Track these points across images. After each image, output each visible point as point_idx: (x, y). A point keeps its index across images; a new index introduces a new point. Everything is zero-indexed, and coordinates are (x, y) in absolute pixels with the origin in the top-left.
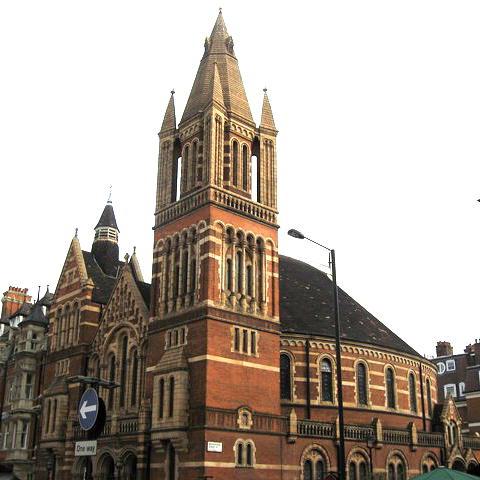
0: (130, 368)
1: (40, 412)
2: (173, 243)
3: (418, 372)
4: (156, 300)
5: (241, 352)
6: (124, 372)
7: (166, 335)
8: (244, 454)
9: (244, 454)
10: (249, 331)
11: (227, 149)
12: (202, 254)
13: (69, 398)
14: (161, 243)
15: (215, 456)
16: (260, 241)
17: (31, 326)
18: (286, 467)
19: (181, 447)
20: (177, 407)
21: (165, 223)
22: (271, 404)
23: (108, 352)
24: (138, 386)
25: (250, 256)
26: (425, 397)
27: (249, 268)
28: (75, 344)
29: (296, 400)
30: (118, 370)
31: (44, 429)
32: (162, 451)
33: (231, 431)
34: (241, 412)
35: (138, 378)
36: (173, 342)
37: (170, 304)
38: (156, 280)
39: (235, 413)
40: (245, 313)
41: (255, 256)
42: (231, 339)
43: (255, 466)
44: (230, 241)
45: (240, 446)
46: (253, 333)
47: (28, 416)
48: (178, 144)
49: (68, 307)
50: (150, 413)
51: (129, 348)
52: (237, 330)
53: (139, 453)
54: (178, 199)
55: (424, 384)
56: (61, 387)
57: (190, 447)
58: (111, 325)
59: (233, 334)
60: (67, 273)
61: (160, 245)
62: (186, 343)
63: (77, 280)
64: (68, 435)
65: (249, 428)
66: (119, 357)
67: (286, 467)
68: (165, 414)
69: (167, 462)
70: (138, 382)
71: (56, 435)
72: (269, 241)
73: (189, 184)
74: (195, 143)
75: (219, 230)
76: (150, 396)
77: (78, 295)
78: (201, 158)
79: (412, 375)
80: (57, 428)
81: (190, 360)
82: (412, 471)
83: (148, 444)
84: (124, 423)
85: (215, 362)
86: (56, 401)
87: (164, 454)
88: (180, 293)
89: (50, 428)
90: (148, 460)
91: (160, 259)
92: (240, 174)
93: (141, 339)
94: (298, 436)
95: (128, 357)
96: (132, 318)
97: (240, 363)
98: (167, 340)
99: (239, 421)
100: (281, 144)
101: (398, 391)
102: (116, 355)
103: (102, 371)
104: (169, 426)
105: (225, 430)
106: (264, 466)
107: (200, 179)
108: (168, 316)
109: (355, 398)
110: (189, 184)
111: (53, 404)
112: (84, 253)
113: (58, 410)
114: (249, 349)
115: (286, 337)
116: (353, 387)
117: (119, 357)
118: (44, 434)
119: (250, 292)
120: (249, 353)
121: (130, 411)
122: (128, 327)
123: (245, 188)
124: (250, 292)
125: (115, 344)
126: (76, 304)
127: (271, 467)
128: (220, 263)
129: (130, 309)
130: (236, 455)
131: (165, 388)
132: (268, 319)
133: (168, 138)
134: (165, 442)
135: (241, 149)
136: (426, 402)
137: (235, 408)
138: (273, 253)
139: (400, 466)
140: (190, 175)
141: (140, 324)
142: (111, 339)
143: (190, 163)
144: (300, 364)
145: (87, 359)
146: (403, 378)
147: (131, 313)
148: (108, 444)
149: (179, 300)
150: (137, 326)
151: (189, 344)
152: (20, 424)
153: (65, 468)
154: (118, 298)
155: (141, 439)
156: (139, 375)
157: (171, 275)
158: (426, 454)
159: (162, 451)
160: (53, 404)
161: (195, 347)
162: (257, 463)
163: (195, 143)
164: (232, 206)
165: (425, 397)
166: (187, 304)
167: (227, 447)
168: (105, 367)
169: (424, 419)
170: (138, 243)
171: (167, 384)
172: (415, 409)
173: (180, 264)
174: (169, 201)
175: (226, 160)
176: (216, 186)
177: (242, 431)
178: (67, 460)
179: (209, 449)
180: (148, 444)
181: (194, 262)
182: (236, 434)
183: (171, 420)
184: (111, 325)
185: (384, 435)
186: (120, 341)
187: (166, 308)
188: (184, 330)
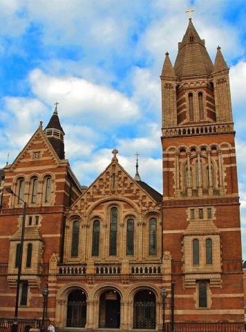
58: (95, 197)
74: (200, 94)
77: (53, 170)
125: (99, 211)
129: (126, 189)
142: (96, 207)
147: (131, 191)
150: (137, 201)
183: (209, 266)
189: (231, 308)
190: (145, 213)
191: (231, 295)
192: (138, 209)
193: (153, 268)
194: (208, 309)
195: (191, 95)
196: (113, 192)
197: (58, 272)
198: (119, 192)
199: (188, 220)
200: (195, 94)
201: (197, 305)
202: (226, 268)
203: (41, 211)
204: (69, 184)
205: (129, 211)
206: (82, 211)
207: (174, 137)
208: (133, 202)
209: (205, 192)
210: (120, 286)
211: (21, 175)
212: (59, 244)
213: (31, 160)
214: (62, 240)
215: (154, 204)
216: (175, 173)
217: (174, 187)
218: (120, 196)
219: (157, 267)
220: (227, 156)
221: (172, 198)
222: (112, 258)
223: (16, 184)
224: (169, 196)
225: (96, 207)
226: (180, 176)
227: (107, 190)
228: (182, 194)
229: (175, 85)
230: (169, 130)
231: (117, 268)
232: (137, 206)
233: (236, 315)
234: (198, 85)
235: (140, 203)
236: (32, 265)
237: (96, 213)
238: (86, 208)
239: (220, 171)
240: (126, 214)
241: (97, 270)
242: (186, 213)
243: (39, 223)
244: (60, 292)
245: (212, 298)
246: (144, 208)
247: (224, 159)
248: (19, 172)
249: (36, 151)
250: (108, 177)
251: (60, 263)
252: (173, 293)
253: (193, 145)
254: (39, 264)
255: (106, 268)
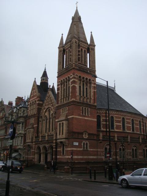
0: (51, 120)
1: (26, 134)
2: (63, 81)
3: (142, 120)
4: (58, 99)
5: (84, 114)
6: (50, 121)
7: (61, 110)
8: (85, 146)
9: (85, 146)
10: (87, 108)
11: (79, 51)
12: (71, 84)
13: (34, 130)
14: (59, 81)
15: (76, 146)
16: (90, 80)
17: (23, 108)
18: (99, 150)
19: (66, 144)
20: (64, 132)
21: (61, 75)
22: (94, 131)
23: (45, 115)
24: (54, 126)
25: (87, 85)
26: (144, 128)
27: (87, 89)
28: (35, 113)
29: (102, 129)
30: (48, 121)
31: (27, 139)
32: (61, 145)
33: (81, 139)
34: (84, 133)
35: (54, 123)
36: (63, 112)
37: (62, 100)
38: (58, 93)
39: (82, 134)
40: (85, 102)
41: (88, 85)
42: (81, 111)
43: (89, 149)
44: (80, 80)
45: (84, 143)
46: (88, 109)
47: (23, 135)
48: (64, 50)
49: (33, 102)
50: (56, 134)
52: (83, 108)
53: (54, 146)
54: (64, 67)
55: (144, 124)
56: (30, 127)
58: (45, 107)
59: (81, 109)
60: (33, 92)
61: (59, 82)
62: (67, 112)
63: (35, 94)
64: (34, 141)
65: (87, 138)
66: (48, 117)
67: (99, 150)
68: (61, 134)
69: (62, 148)
70: (54, 124)
71: (30, 141)
72: (93, 80)
73: (68, 63)
74: (69, 50)
75: (76, 77)
76: (56, 129)
77: (36, 98)
78: (71, 55)
79: (140, 121)
80: (30, 139)
81: (68, 117)
82: (140, 151)
83: (56, 143)
84: (49, 137)
85: (76, 118)
86: (30, 131)
87: (61, 146)
88: (65, 97)
89: (29, 139)
90: (56, 148)
91: (59, 86)
92: (83, 59)
93: (54, 111)
94: (103, 140)
95: (51, 117)
96: (52, 105)
97: (83, 118)
99: (84, 136)
100: (96, 49)
101: (135, 126)
102: (47, 116)
103: (43, 121)
104: (62, 138)
105: (79, 139)
106: (92, 150)
107: (71, 61)
108: (62, 104)
109: (121, 128)
110: (68, 63)
111: (29, 131)
112: (38, 86)
113: (31, 133)
114: (87, 114)
115: (100, 110)
116: (121, 125)
117: (48, 117)
118: (27, 140)
119: (87, 96)
120: (87, 115)
121: (51, 133)
122: (50, 108)
123: (85, 63)
124: (87, 96)
126: (35, 101)
127: (94, 150)
128: (77, 87)
130: (83, 146)
131: (61, 126)
132: (93, 104)
133: (61, 49)
134: (61, 142)
135: (83, 51)
136: (145, 130)
137: (82, 132)
138: (95, 84)
139: (136, 149)
140: (68, 60)
141: (54, 107)
143: (68, 56)
144: (104, 118)
145: (39, 118)
146: (137, 122)
147: (51, 103)
148: (45, 143)
149: (65, 99)
150: (53, 107)
152: (20, 137)
153: (33, 150)
154: (47, 99)
155: (54, 142)
156: (54, 122)
157: (63, 91)
158: (144, 146)
159: (61, 145)
160: (29, 131)
162: (90, 148)
163: (69, 50)
164: (81, 69)
165: (144, 128)
166: (67, 100)
167: (80, 144)
168: (44, 120)
169: (144, 135)
170: (53, 81)
171: (61, 125)
172: (141, 132)
173: (65, 88)
174: (62, 68)
175: (79, 55)
176: (75, 63)
177: (84, 139)
178: (33, 148)
179: (74, 144)
180: (56, 143)
181: (69, 87)
182: (83, 140)
184: (45, 107)
185: (131, 140)
186: (48, 112)
187: (61, 101)
188: (66, 108)
194: (64, 156)
195: (67, 52)
198: (49, 104)
201: (62, 154)
220: (71, 81)
221: (58, 105)
244: (36, 148)
245: (66, 151)
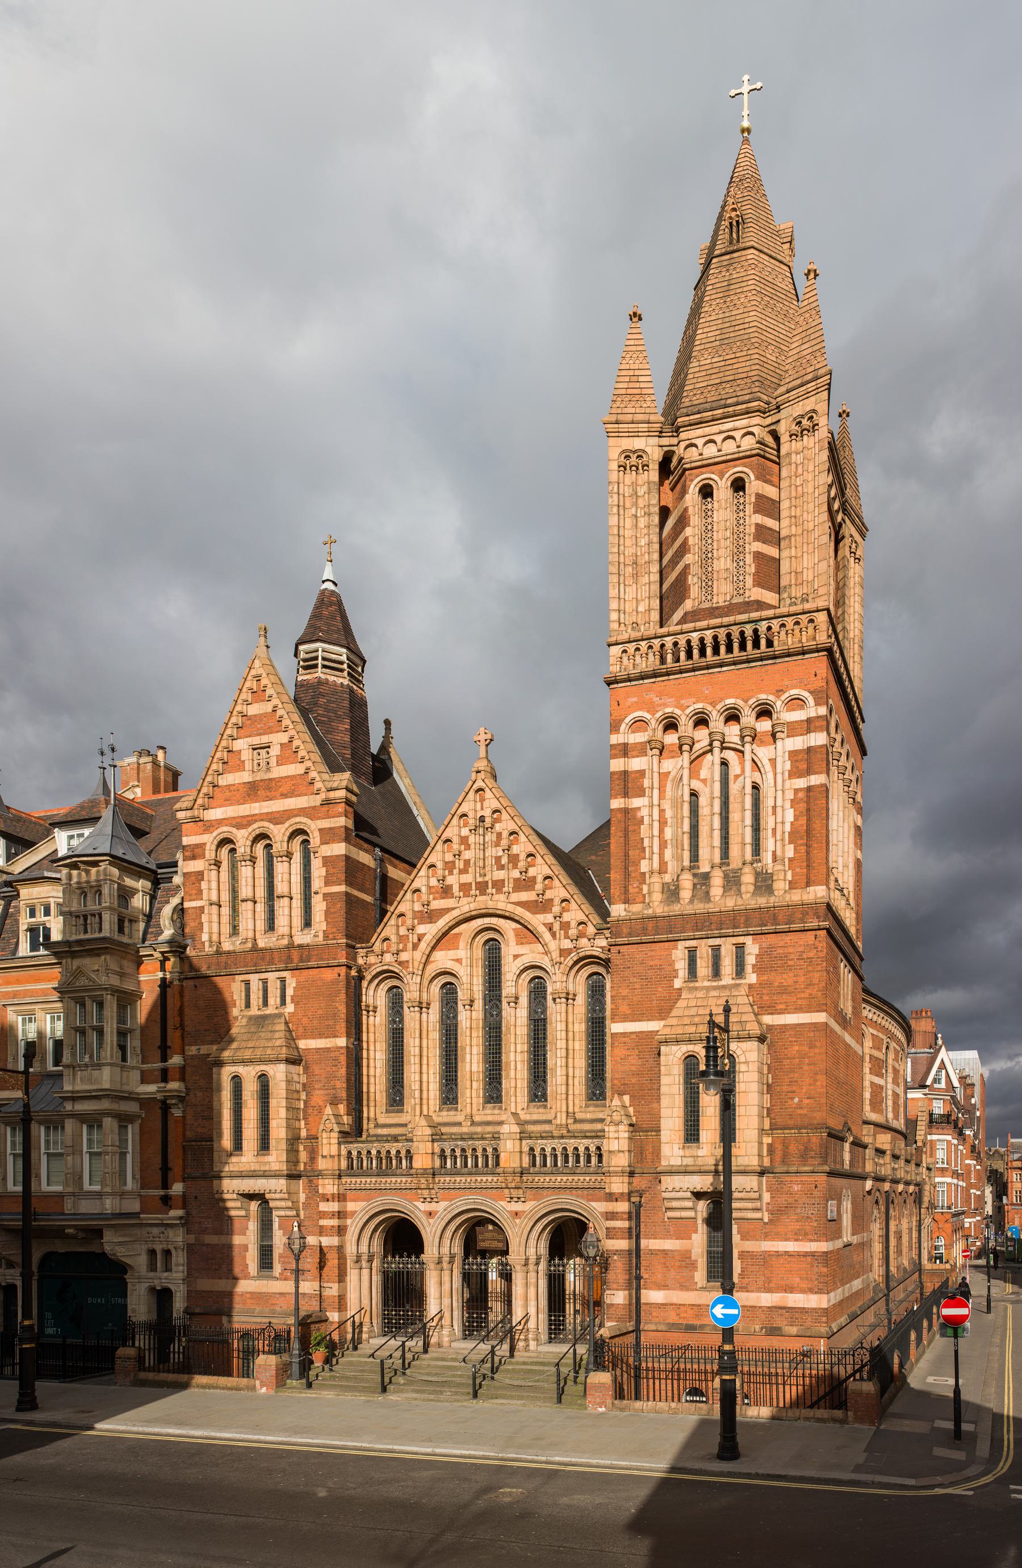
32: (691, 1214)
51: (510, 969)
57: (778, 1212)
58: (437, 904)
62: (752, 978)
74: (738, 485)
77: (309, 812)
81: (768, 1019)
96: (525, 896)
98: (681, 966)
125: (452, 954)
129: (516, 874)
142: (441, 940)
147: (525, 883)
150: (549, 918)
151: (761, 984)
155: (618, 1185)
161: (783, 990)
188: (740, 948)
189: (790, 1289)
190: (569, 961)
191: (791, 1246)
192: (553, 945)
193: (581, 1149)
196: (482, 888)
197: (344, 1164)
198: (499, 885)
199: (678, 983)
200: (723, 490)
202: (779, 1154)
203: (289, 959)
204: (366, 858)
205: (531, 954)
206: (404, 956)
207: (642, 677)
208: (537, 921)
209: (732, 882)
210: (502, 1208)
211: (225, 831)
212: (343, 1071)
213: (245, 777)
214: (355, 1058)
215: (591, 930)
216: (644, 812)
217: (644, 866)
218: (500, 902)
219: (593, 1148)
220: (798, 743)
221: (636, 908)
222: (490, 1113)
223: (218, 864)
224: (626, 901)
225: (441, 940)
226: (663, 823)
227: (467, 878)
228: (672, 893)
229: (656, 455)
230: (631, 647)
231: (490, 1150)
232: (547, 936)
233: (803, 1310)
234: (730, 447)
235: (556, 927)
236: (273, 1143)
237: (442, 959)
238: (415, 947)
239: (779, 803)
240: (520, 963)
241: (443, 1156)
242: (672, 964)
243: (288, 999)
244: (353, 1226)
246: (567, 944)
247: (793, 754)
248: (220, 822)
249: (256, 740)
250: (465, 832)
251: (354, 1132)
252: (635, 1234)
253: (700, 705)
254: (293, 1140)
255: (463, 1150)
